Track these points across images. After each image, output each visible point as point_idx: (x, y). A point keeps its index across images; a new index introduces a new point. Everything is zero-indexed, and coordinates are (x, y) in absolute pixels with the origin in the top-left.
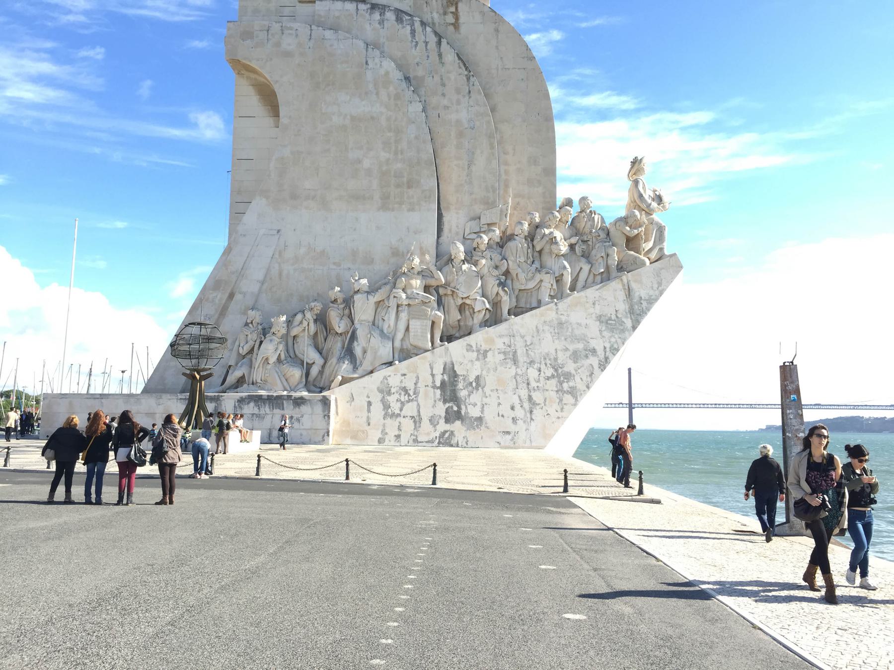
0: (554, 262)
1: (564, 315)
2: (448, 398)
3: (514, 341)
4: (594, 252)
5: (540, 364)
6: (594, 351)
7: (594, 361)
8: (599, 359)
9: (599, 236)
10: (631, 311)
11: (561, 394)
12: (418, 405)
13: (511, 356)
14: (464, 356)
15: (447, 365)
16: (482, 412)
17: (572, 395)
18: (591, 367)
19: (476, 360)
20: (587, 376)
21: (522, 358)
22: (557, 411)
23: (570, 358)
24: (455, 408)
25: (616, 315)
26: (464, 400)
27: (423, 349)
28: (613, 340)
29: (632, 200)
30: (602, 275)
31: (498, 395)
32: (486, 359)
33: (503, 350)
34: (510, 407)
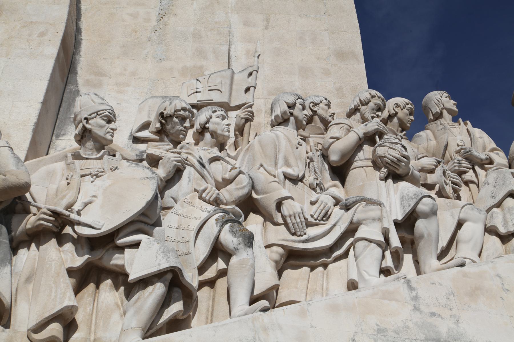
4: (485, 191)
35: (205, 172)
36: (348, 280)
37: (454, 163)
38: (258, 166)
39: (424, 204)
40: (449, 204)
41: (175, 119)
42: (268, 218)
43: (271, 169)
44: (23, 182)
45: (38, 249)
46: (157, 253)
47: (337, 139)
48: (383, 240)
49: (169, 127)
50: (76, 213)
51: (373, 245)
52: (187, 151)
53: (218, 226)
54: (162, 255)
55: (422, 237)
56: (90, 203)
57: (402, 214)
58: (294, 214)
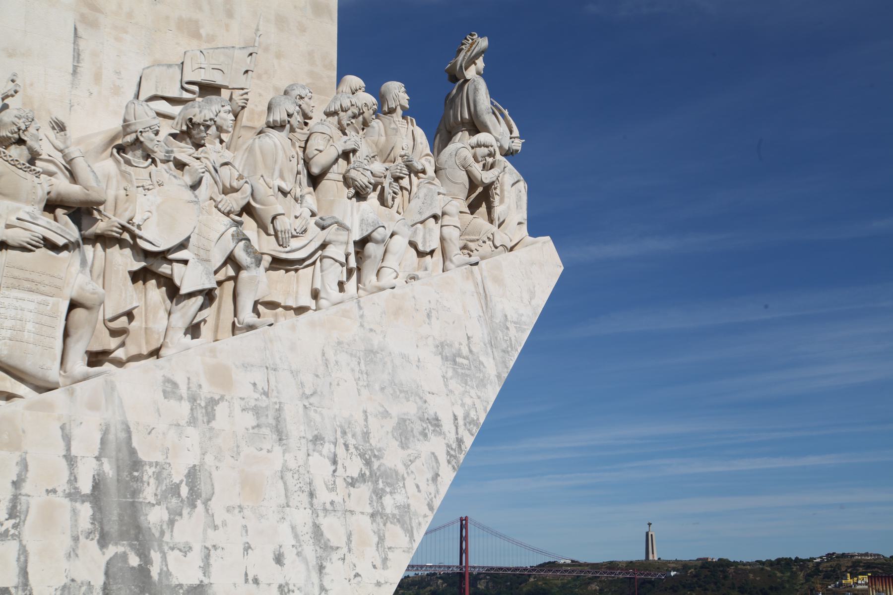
0: (349, 209)
1: (375, 331)
2: (113, 528)
3: (276, 382)
5: (335, 444)
6: (436, 422)
7: (437, 445)
8: (447, 442)
9: (424, 172)
10: (492, 343)
11: (381, 525)
12: (23, 551)
13: (271, 421)
14: (158, 410)
15: (112, 430)
16: (206, 568)
17: (402, 527)
18: (433, 457)
19: (189, 423)
20: (428, 480)
21: (296, 429)
22: (374, 567)
23: (393, 435)
24: (134, 561)
25: (469, 347)
26: (157, 535)
27: (32, 384)
28: (468, 401)
29: (467, 116)
30: (432, 257)
31: (244, 522)
32: (213, 424)
33: (252, 403)
34: (272, 556)
35: (218, 179)
36: (314, 287)
37: (397, 169)
38: (259, 176)
39: (379, 234)
40: (388, 216)
41: (202, 128)
42: (262, 226)
43: (268, 180)
44: (103, 200)
45: (104, 250)
46: (202, 273)
47: (321, 151)
48: (345, 262)
49: (194, 132)
50: (136, 227)
51: (338, 264)
52: (206, 155)
53: (235, 242)
54: (205, 275)
55: (369, 257)
56: (148, 219)
57: (360, 236)
58: (285, 230)
